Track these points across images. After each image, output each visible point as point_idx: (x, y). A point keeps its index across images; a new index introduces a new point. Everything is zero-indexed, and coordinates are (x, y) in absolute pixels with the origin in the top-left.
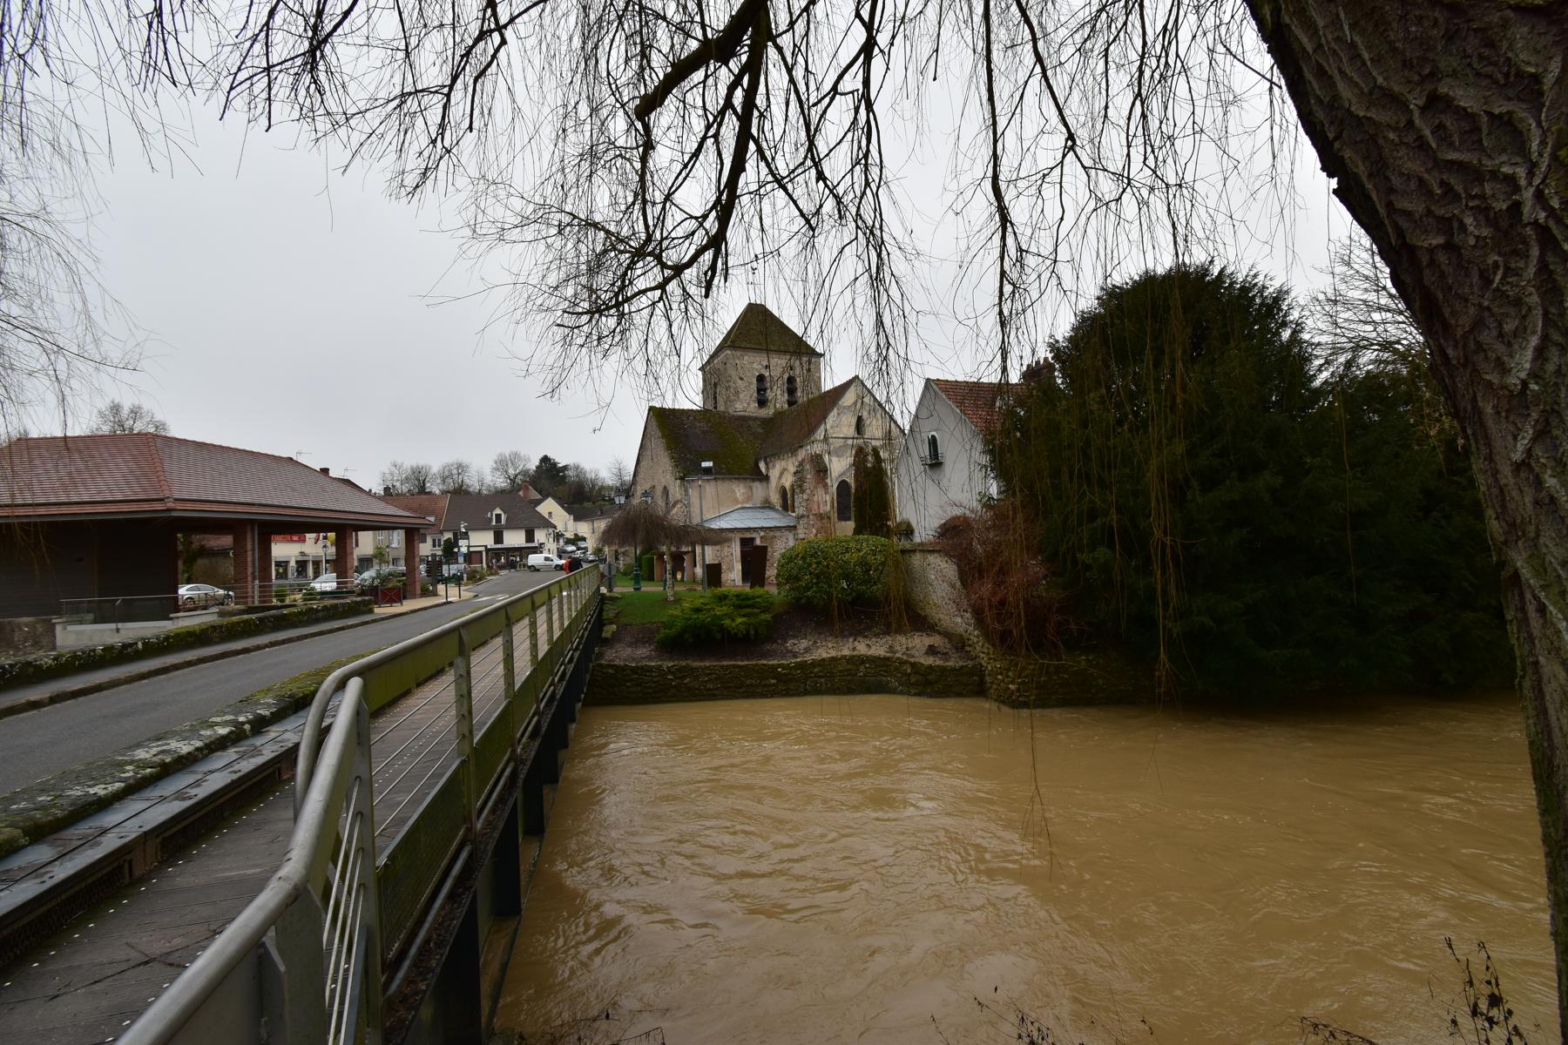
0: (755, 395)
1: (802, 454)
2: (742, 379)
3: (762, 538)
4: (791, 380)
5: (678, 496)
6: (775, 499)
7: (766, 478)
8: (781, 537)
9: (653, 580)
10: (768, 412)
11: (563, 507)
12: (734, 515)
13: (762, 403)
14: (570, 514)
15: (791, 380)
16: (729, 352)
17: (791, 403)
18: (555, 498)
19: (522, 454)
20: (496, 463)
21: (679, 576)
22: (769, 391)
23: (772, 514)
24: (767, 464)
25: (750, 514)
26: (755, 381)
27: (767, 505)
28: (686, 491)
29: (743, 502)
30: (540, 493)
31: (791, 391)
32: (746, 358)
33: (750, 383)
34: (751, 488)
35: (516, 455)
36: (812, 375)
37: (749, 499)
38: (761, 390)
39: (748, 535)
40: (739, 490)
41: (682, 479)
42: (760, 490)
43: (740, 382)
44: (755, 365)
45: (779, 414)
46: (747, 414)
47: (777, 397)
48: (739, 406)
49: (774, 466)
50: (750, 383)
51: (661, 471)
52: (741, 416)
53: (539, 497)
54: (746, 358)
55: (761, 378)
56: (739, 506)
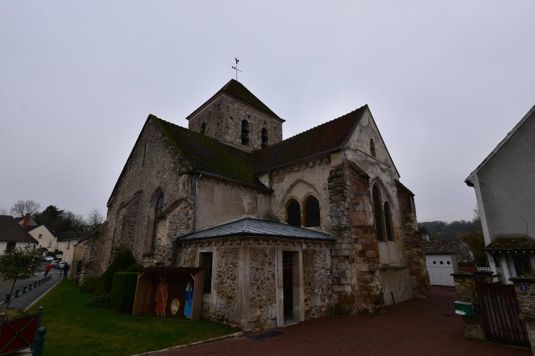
0: (240, 133)
1: (337, 160)
2: (232, 118)
3: (304, 252)
4: (264, 131)
5: (181, 193)
6: (281, 213)
7: (269, 192)
8: (320, 252)
9: (130, 311)
10: (248, 149)
11: (51, 232)
12: (245, 223)
13: (245, 141)
14: (55, 236)
15: (264, 131)
16: (224, 96)
17: (263, 146)
18: (47, 226)
19: (35, 202)
20: (16, 206)
21: (175, 308)
22: (250, 134)
23: (281, 227)
24: (271, 178)
25: (257, 225)
26: (241, 123)
27: (270, 219)
28: (193, 188)
29: (249, 213)
30: (37, 222)
31: (264, 139)
32: (235, 105)
33: (238, 124)
34: (256, 199)
35: (32, 203)
36: (278, 129)
37: (254, 210)
38: (245, 131)
39: (291, 248)
40: (246, 200)
41: (191, 174)
42: (263, 203)
43: (230, 120)
44: (241, 112)
45: (256, 153)
46: (232, 145)
47: (256, 142)
48: (228, 138)
49: (281, 180)
50: (238, 124)
51: (154, 173)
52: (229, 146)
53: (36, 224)
54: (235, 105)
55: (245, 123)
56: (245, 216)
